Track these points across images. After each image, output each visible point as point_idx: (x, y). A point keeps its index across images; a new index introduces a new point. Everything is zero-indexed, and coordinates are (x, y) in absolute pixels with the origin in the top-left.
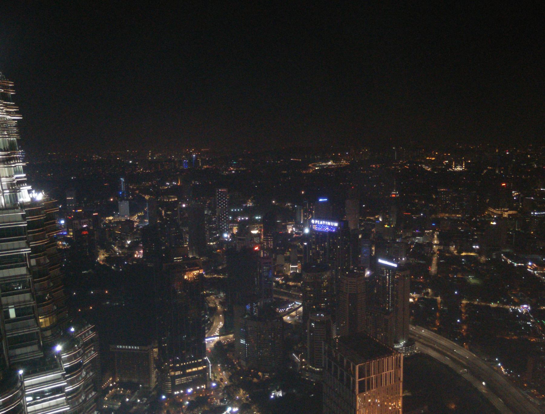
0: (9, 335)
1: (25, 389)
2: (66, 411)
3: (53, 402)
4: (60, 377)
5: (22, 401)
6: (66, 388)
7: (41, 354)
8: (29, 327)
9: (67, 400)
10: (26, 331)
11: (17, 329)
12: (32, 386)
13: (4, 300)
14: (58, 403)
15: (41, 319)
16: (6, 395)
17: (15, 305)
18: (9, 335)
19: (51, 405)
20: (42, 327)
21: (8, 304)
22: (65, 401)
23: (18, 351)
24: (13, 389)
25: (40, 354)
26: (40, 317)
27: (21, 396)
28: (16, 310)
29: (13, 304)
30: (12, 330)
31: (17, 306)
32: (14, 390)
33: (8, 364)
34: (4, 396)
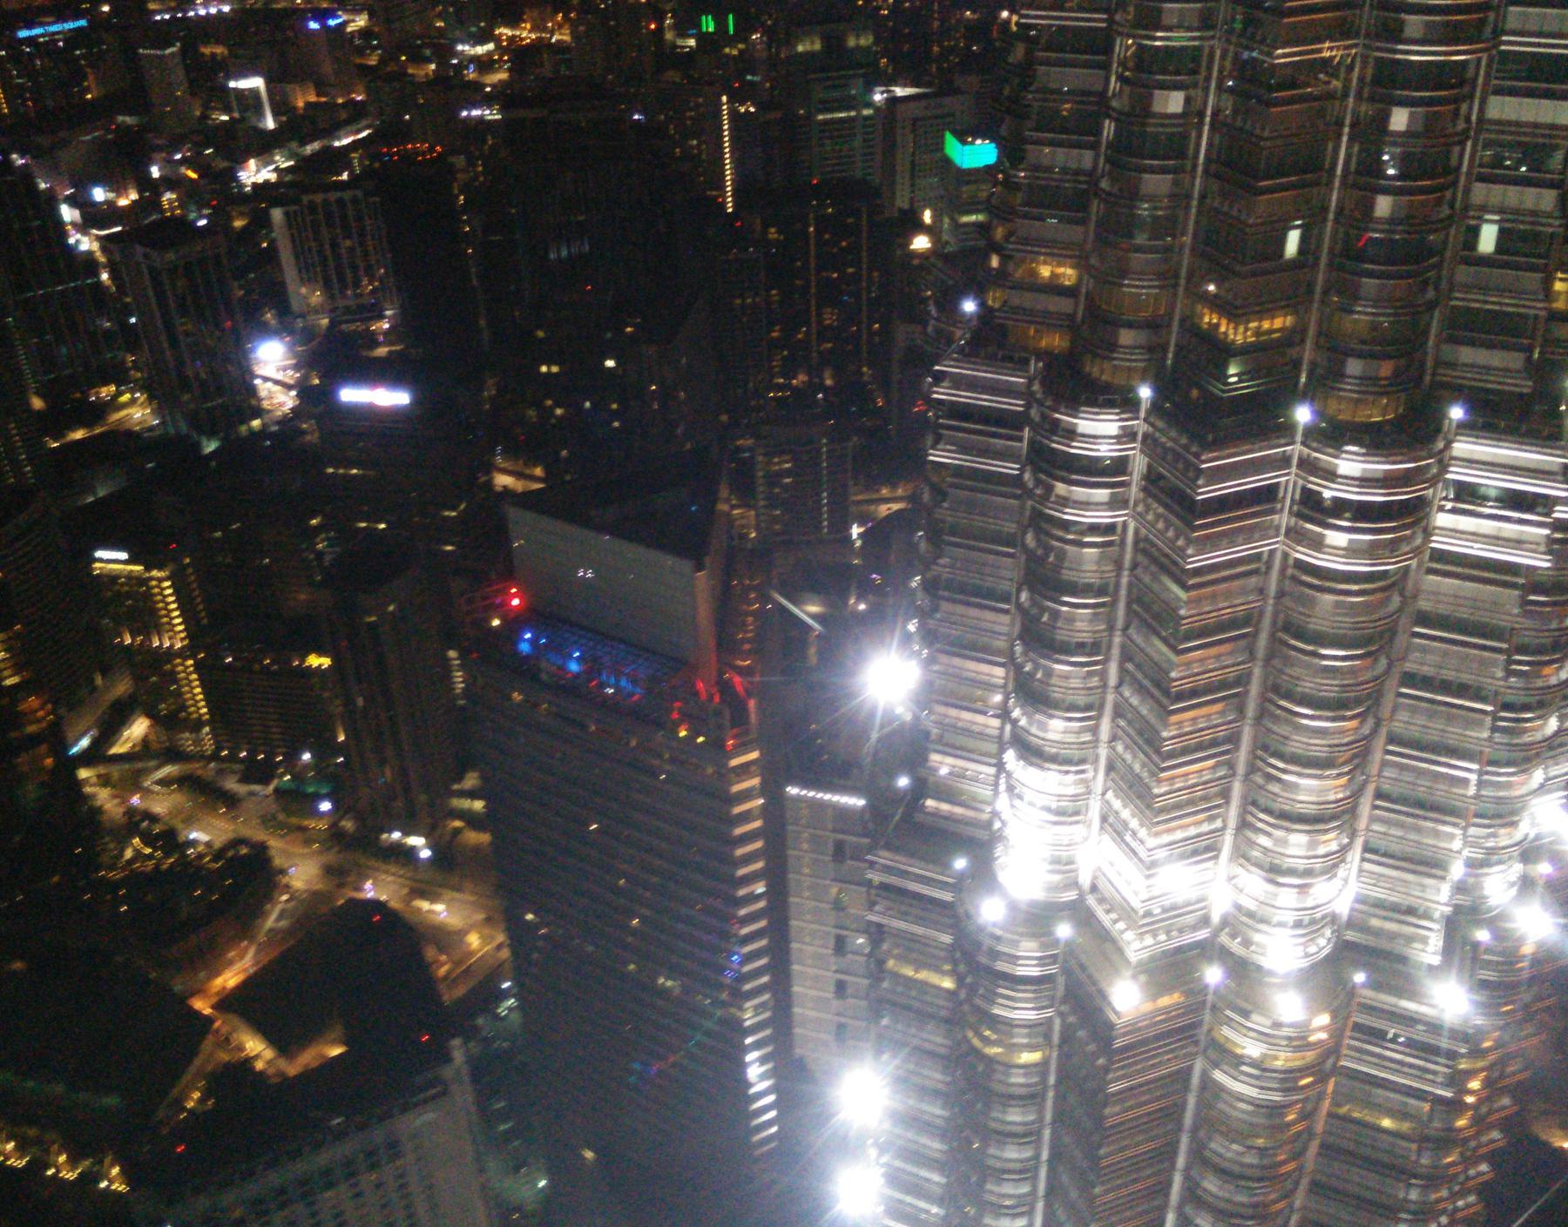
0: (1457, 299)
1: (1449, 465)
2: (1535, 568)
3: (1509, 529)
4: (1555, 469)
5: (1431, 491)
6: (1557, 508)
7: (1526, 386)
8: (1517, 293)
9: (1551, 541)
10: (1509, 304)
11: (1484, 289)
12: (1471, 462)
13: (1480, 192)
14: (1524, 538)
15: (1561, 280)
16: (1399, 458)
17: (1505, 216)
18: (1457, 299)
19: (1505, 534)
20: (1555, 305)
21: (1484, 209)
22: (1543, 541)
23: (1467, 354)
24: (1422, 450)
25: (1523, 383)
26: (1560, 275)
27: (1434, 477)
28: (1503, 234)
29: (1500, 211)
30: (1467, 288)
31: (1507, 221)
32: (1424, 454)
33: (1427, 378)
34: (1392, 459)
